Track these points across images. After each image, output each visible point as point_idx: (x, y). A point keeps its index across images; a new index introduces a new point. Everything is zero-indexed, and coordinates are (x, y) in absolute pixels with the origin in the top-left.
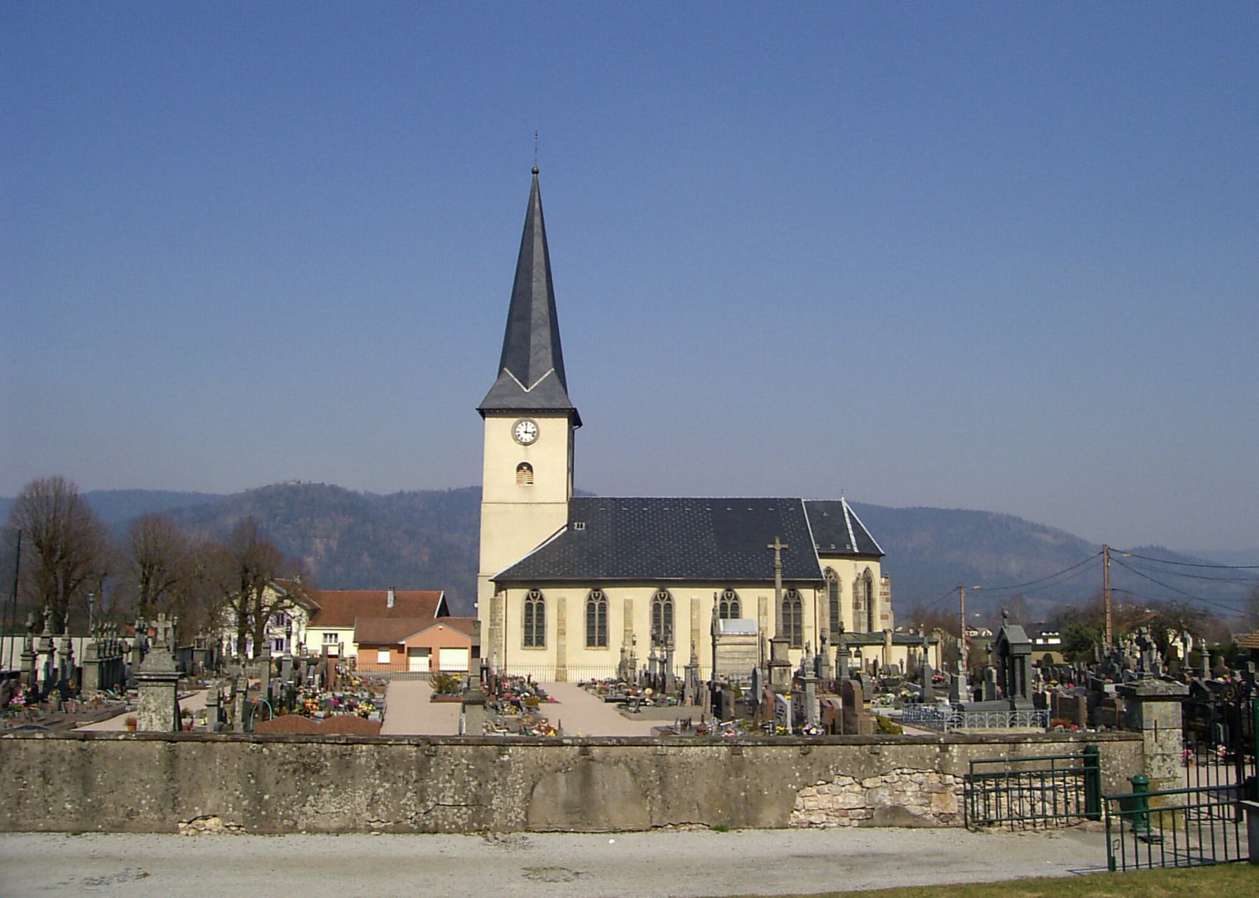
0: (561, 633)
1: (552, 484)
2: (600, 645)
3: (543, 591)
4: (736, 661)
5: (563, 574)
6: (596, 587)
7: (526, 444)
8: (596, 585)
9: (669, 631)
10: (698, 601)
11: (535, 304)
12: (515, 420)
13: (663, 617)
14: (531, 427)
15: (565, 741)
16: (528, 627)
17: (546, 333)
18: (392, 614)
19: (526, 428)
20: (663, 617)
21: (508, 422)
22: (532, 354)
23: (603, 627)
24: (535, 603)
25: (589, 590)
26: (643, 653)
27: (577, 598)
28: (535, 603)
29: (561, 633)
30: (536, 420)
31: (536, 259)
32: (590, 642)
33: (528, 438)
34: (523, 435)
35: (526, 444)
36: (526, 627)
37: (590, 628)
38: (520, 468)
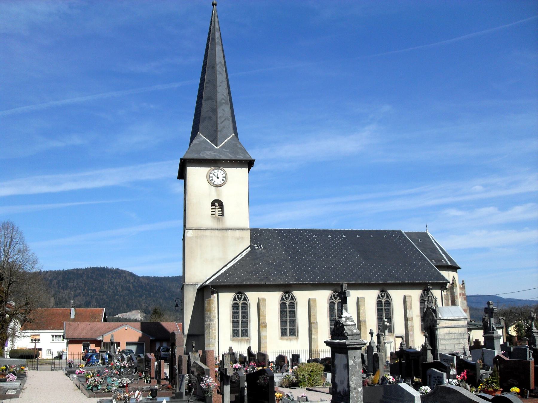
0: (261, 326)
1: (239, 214)
2: (290, 335)
3: (390, 292)
4: (453, 342)
5: (261, 280)
6: (287, 290)
7: (217, 186)
8: (383, 287)
9: (390, 319)
10: (264, 300)
11: (219, 89)
12: (209, 168)
13: (384, 310)
14: (220, 173)
15: (9, 393)
16: (235, 322)
17: (227, 109)
18: (74, 320)
19: (219, 174)
20: (384, 310)
21: (205, 170)
22: (219, 121)
23: (293, 322)
24: (240, 303)
25: (281, 293)
26: (418, 341)
27: (273, 299)
28: (240, 303)
29: (261, 326)
30: (225, 169)
31: (218, 60)
32: (283, 333)
33: (219, 181)
34: (215, 179)
35: (217, 186)
36: (233, 322)
37: (283, 322)
38: (213, 204)
